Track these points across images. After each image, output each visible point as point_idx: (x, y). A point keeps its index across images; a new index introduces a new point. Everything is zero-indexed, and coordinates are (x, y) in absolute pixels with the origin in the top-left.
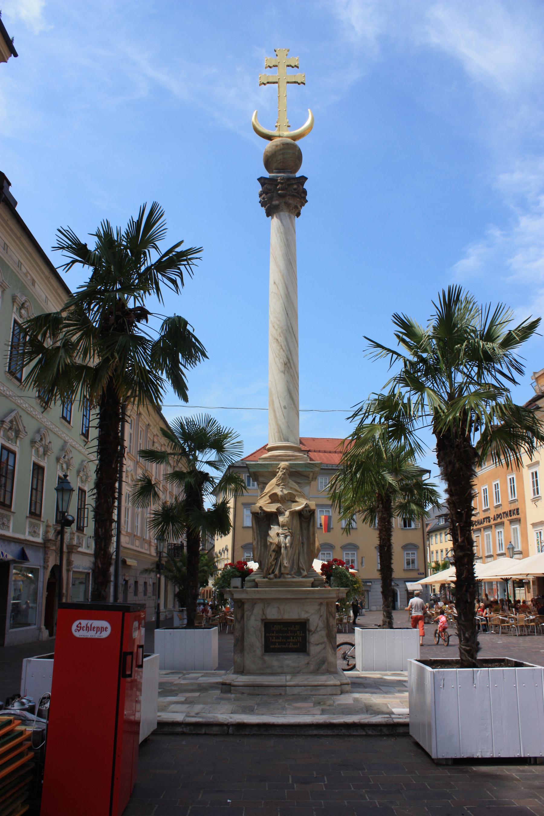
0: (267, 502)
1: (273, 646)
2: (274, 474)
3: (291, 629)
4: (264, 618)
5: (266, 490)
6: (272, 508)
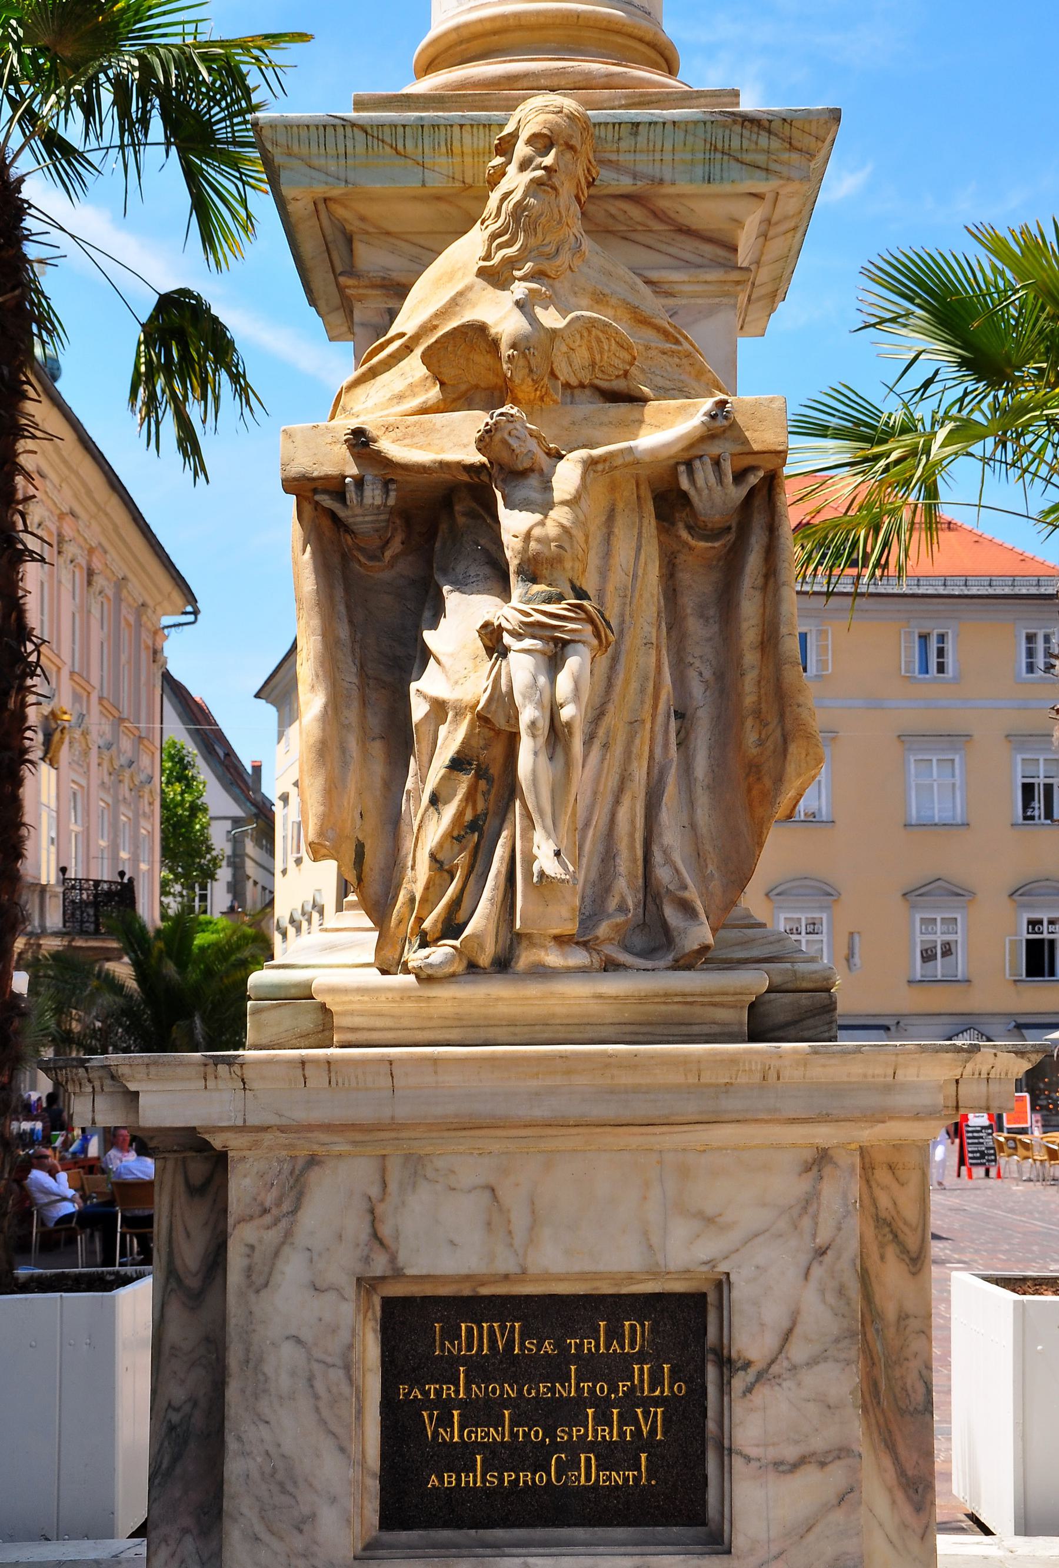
0: (415, 403)
1: (449, 1479)
3: (589, 1345)
4: (379, 1266)
5: (409, 319)
6: (454, 440)
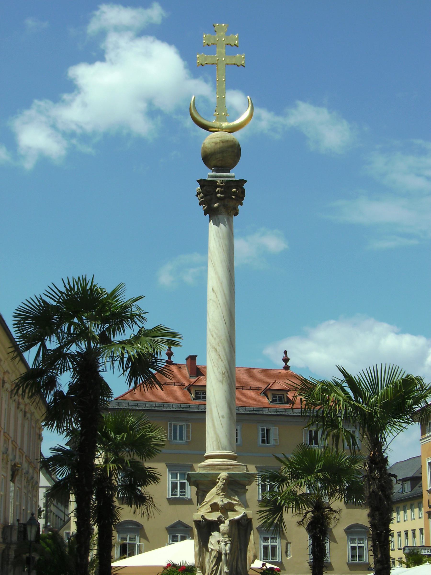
0: (208, 511)
2: (214, 484)
5: (207, 499)
6: (214, 517)
